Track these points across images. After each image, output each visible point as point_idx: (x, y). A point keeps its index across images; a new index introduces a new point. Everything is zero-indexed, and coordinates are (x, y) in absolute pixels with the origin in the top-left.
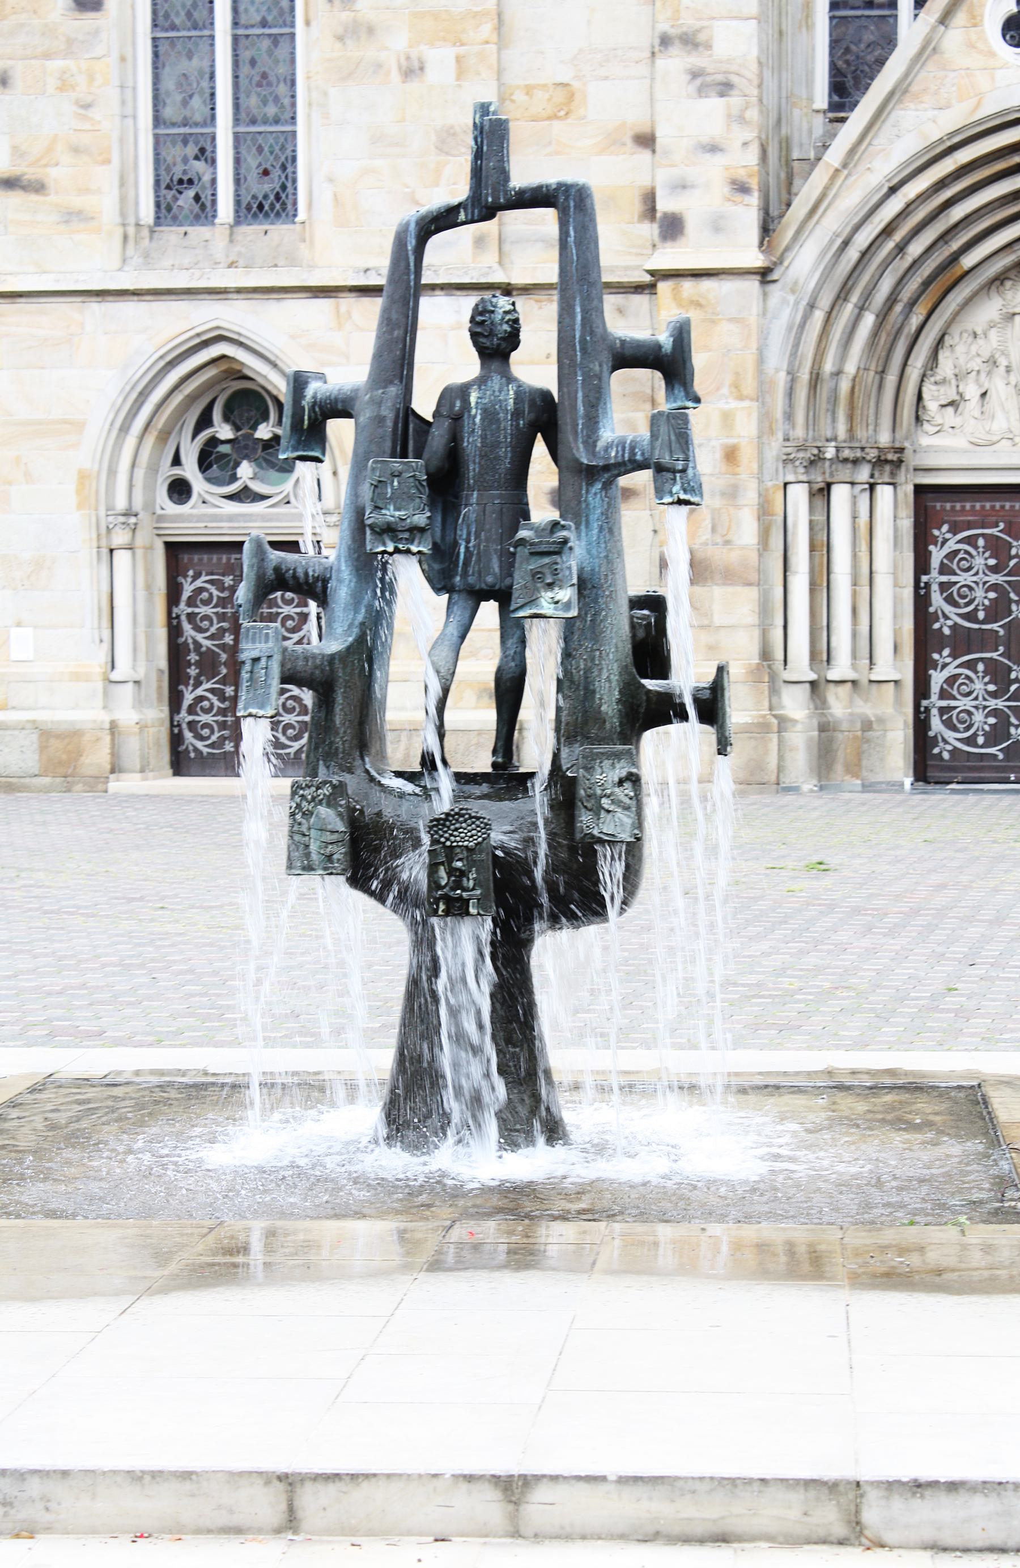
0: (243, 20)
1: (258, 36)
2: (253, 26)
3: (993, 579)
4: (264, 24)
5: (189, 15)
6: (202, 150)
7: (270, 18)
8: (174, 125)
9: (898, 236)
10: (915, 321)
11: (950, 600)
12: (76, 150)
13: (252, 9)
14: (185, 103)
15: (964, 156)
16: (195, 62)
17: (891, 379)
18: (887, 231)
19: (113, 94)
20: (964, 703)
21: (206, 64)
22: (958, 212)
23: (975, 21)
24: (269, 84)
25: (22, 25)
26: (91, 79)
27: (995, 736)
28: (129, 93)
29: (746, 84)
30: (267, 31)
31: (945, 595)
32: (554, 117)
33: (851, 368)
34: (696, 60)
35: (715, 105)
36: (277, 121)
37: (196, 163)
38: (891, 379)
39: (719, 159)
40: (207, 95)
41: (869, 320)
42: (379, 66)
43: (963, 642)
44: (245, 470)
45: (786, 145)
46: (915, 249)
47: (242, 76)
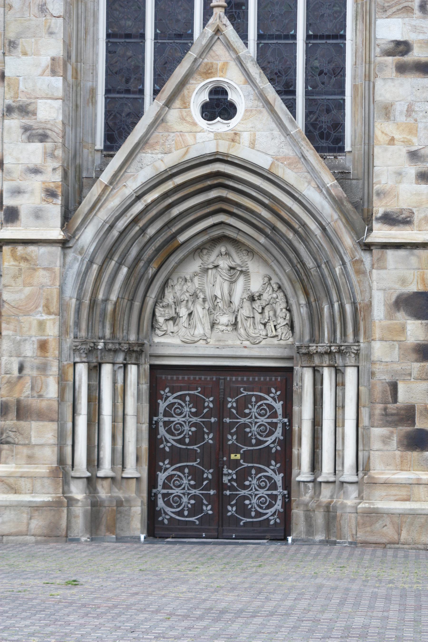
3: (194, 420)
9: (141, 224)
10: (151, 272)
11: (169, 432)
15: (179, 180)
17: (137, 304)
18: (135, 220)
20: (176, 491)
22: (176, 211)
23: (186, 105)
27: (195, 510)
29: (56, 134)
31: (274, 410)
33: (113, 297)
34: (26, 121)
38: (137, 304)
41: (124, 270)
43: (176, 455)
45: (79, 169)
46: (151, 231)
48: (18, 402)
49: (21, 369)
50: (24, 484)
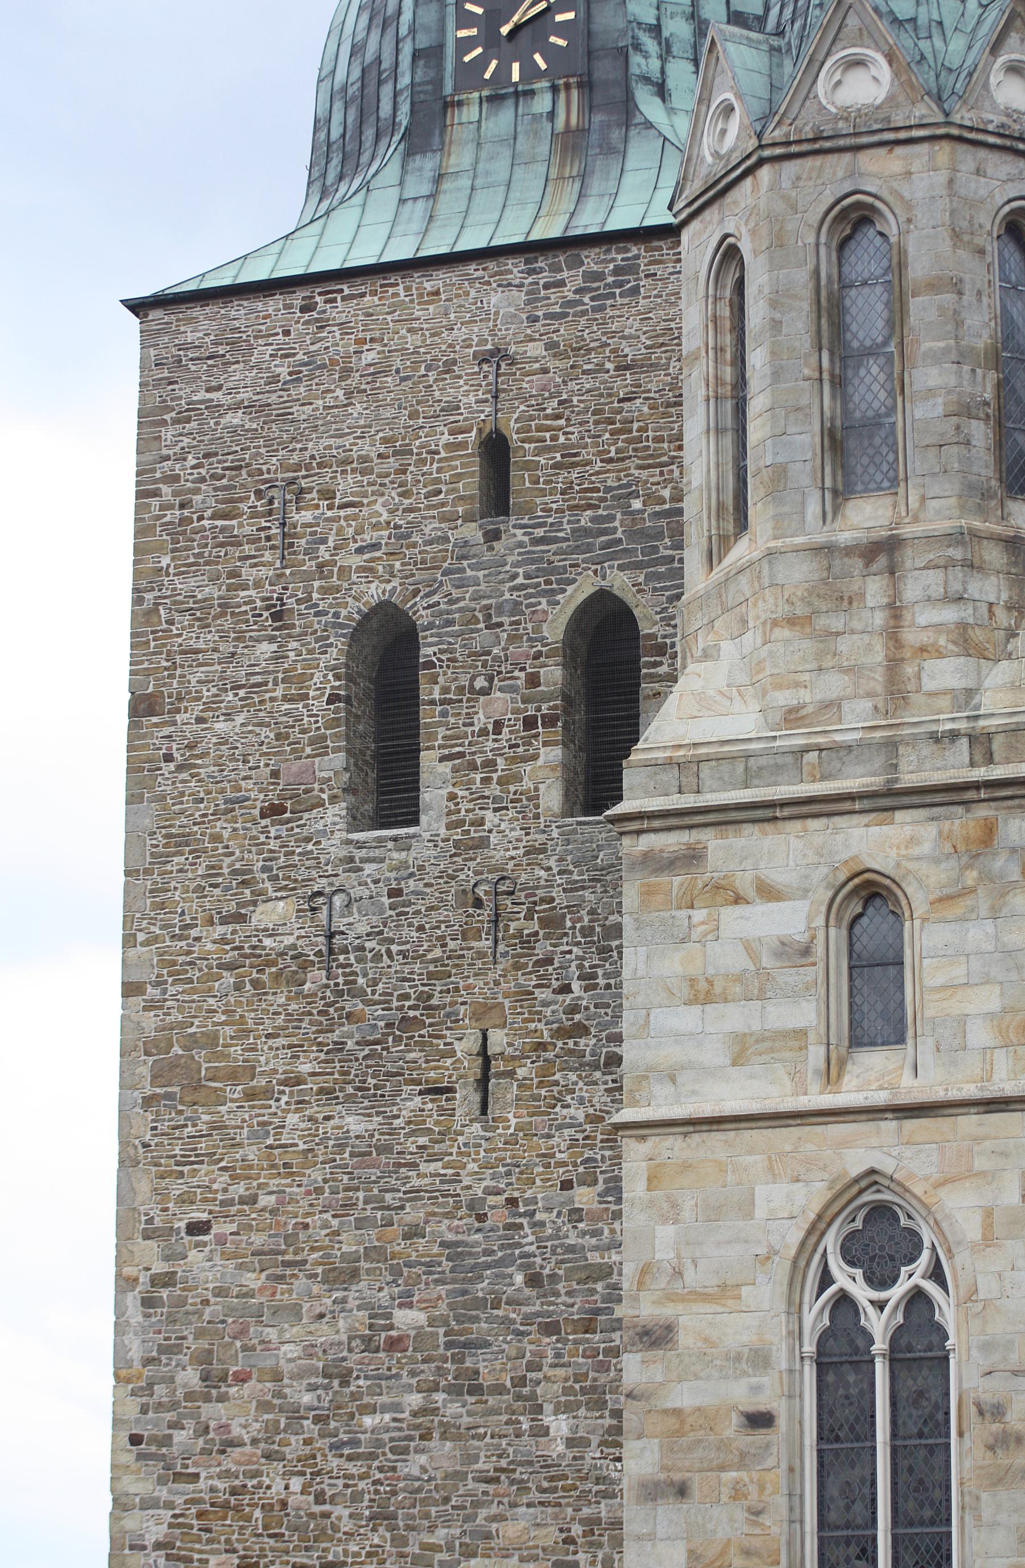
0: (901, 1432)
1: (915, 1446)
2: (910, 1438)
4: (921, 1435)
5: (852, 1428)
6: (864, 1551)
7: (926, 1430)
8: (837, 1528)
12: (747, 1553)
13: (910, 1422)
14: (848, 1508)
16: (857, 1471)
19: (782, 1501)
21: (867, 1472)
24: (926, 1490)
25: (700, 1441)
26: (762, 1488)
28: (796, 1500)
30: (923, 1442)
36: (932, 1523)
37: (858, 1563)
40: (868, 1501)
47: (900, 1482)
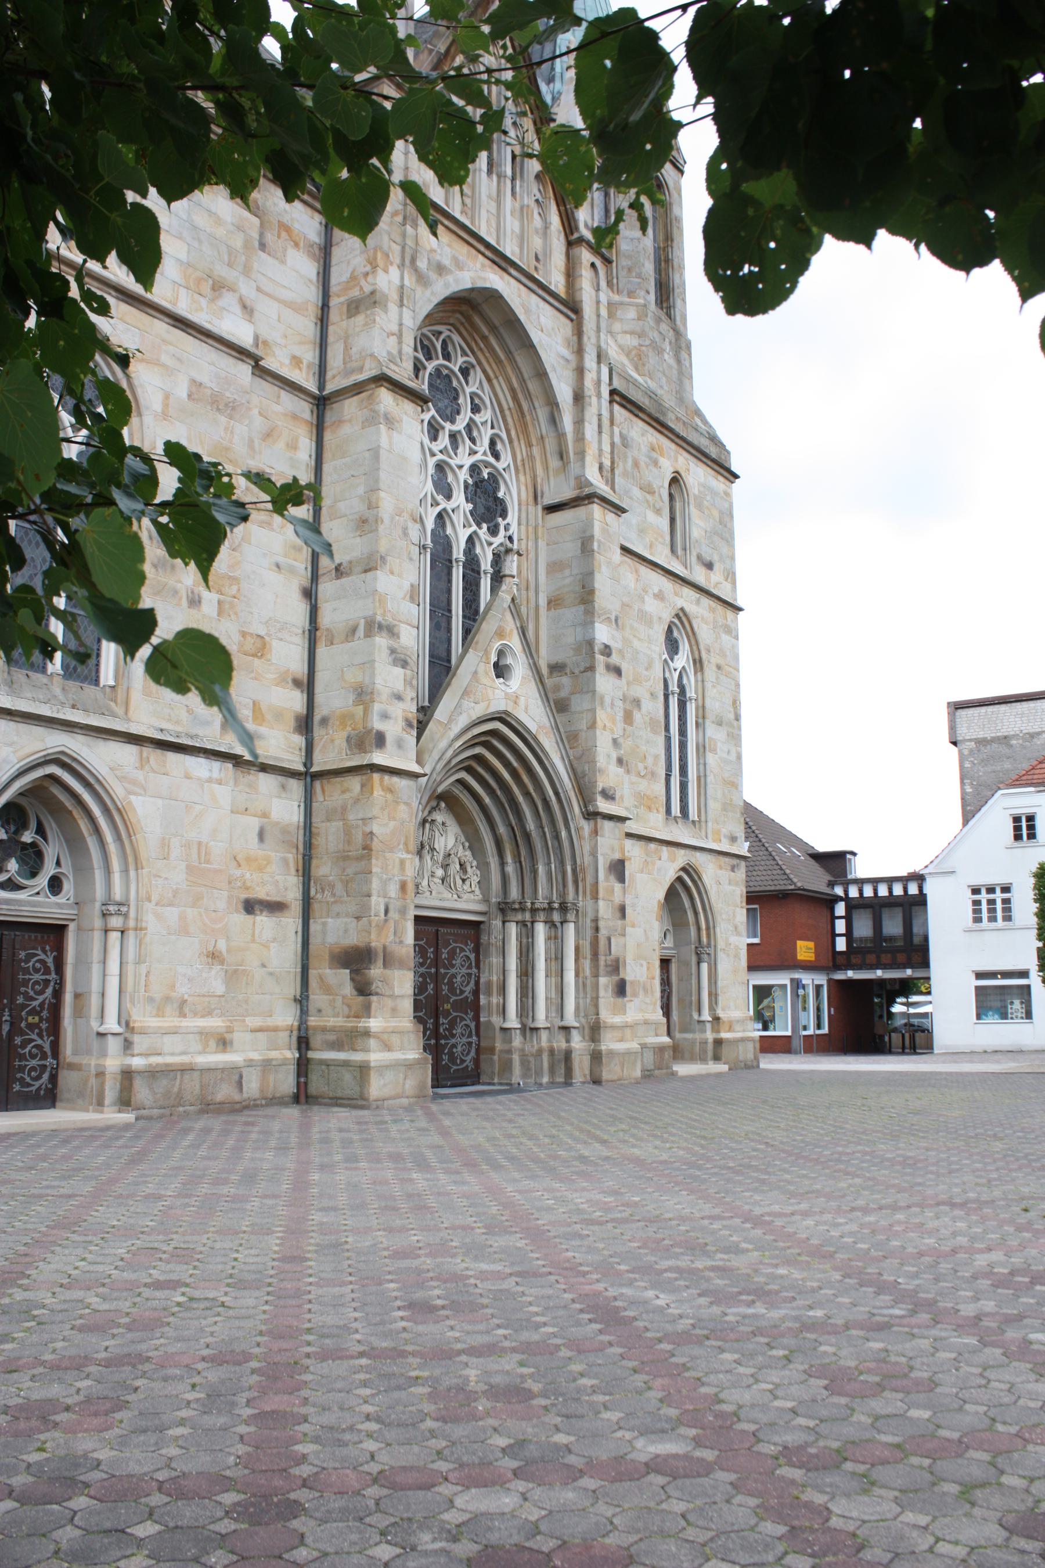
32: (254, 655)
35: (399, 671)
39: (401, 705)
42: (176, 592)
44: (13, 865)
48: (385, 948)
49: (386, 912)
50: (395, 1040)
